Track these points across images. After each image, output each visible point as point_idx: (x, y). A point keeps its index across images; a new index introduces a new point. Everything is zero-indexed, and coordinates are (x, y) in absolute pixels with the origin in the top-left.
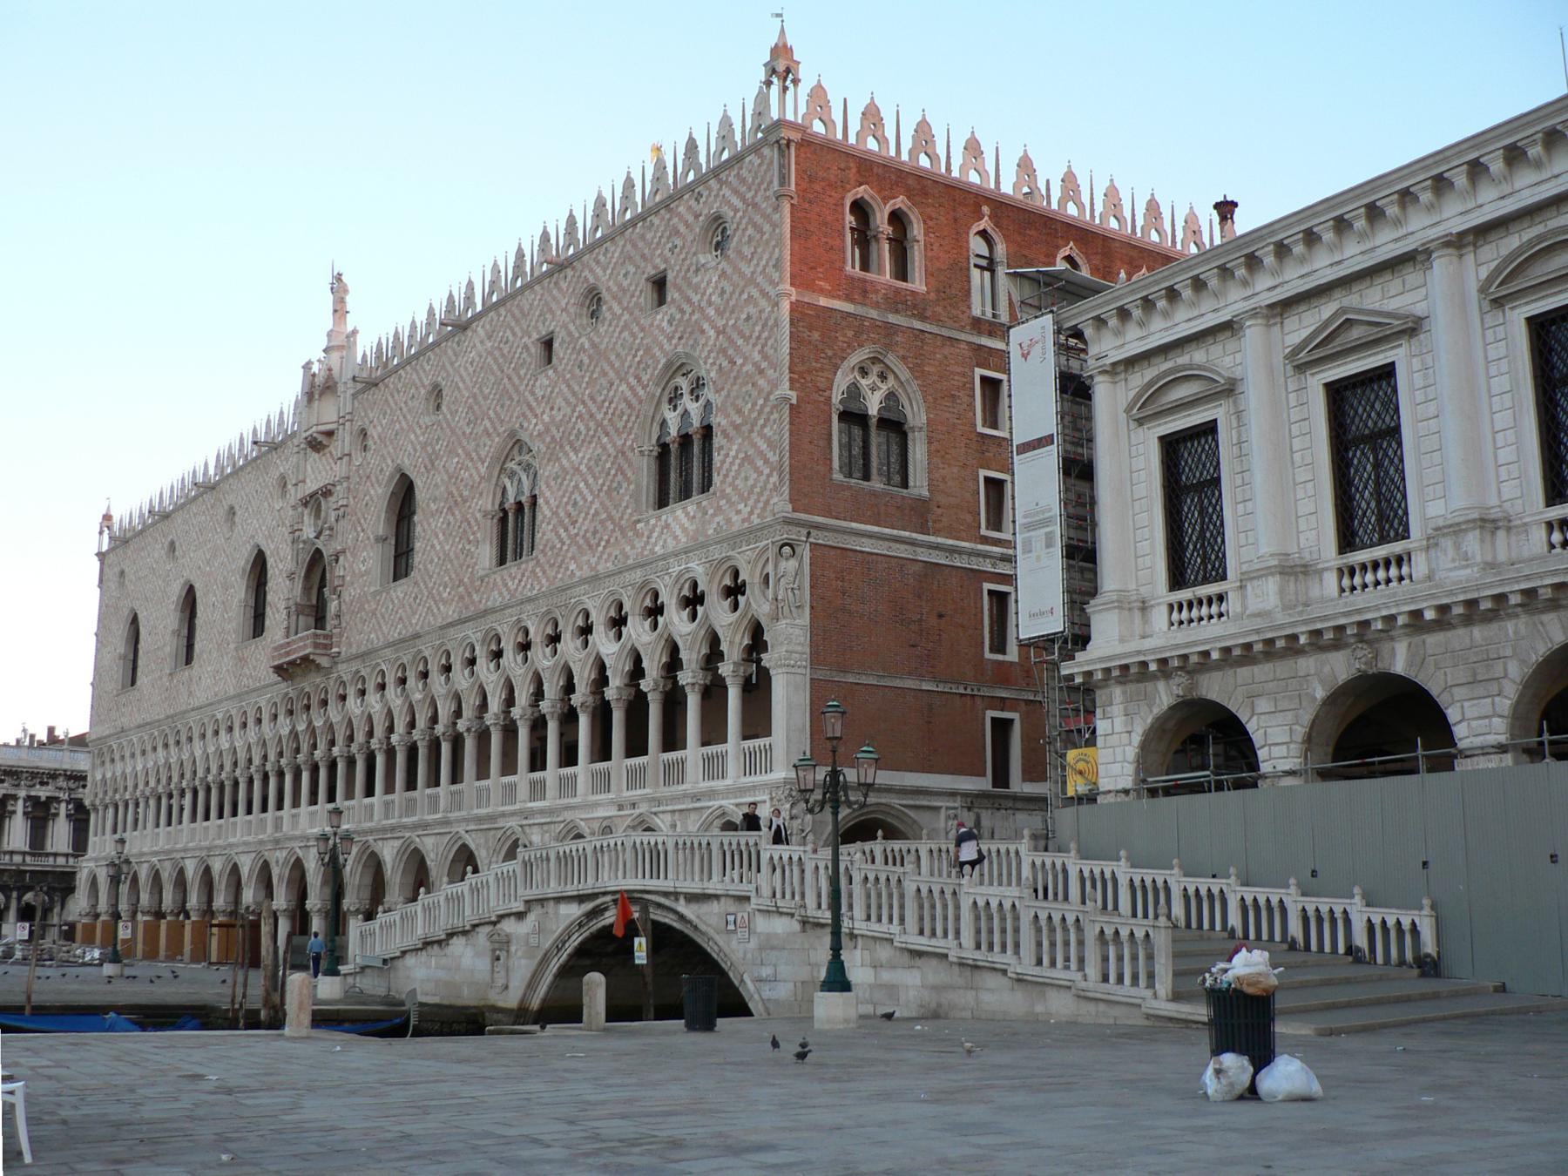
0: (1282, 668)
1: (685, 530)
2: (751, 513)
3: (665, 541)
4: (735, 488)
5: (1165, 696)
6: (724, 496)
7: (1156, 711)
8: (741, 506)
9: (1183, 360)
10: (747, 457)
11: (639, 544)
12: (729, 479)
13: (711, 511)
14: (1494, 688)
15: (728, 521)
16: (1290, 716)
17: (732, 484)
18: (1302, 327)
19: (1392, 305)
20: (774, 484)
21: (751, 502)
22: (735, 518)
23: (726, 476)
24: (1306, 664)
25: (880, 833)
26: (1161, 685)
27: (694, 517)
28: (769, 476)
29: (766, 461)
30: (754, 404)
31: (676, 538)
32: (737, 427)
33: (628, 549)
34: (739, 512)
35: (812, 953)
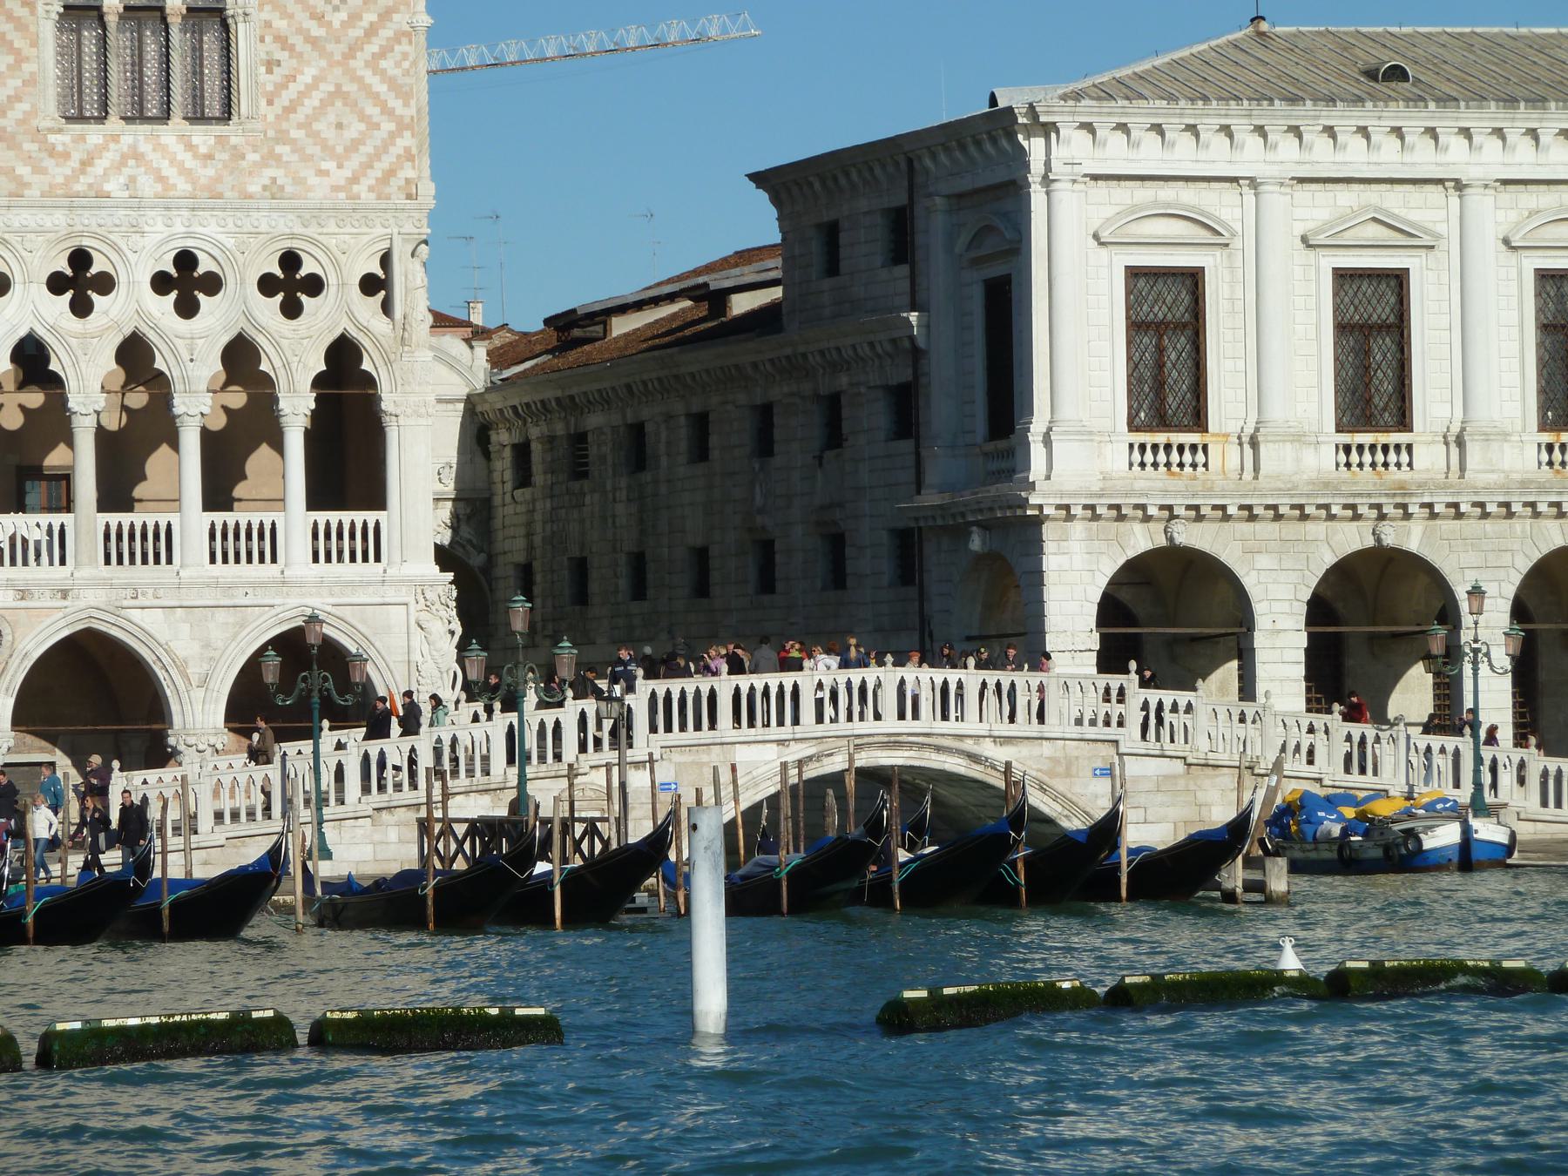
0: (1291, 529)
1: (184, 171)
2: (354, 180)
3: (132, 179)
4: (314, 135)
5: (1141, 539)
6: (282, 137)
7: (1131, 554)
8: (329, 165)
9: (1167, 193)
10: (338, 93)
11: (58, 173)
12: (300, 116)
13: (253, 157)
14: (1502, 574)
15: (299, 181)
16: (1293, 577)
17: (306, 125)
18: (1318, 209)
19: (1414, 216)
20: (407, 150)
21: (354, 163)
22: (313, 180)
23: (290, 109)
24: (1316, 529)
25: (1026, 666)
26: (1138, 528)
27: (209, 157)
28: (393, 136)
29: (388, 112)
30: (354, 17)
31: (161, 179)
32: (314, 42)
33: (23, 170)
34: (326, 173)
35: (1199, 794)
